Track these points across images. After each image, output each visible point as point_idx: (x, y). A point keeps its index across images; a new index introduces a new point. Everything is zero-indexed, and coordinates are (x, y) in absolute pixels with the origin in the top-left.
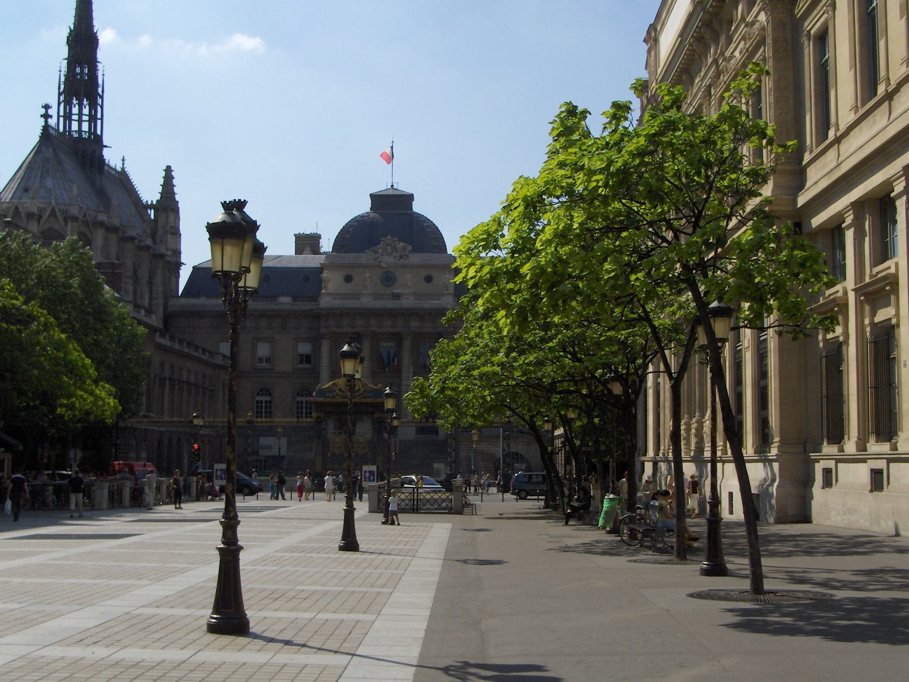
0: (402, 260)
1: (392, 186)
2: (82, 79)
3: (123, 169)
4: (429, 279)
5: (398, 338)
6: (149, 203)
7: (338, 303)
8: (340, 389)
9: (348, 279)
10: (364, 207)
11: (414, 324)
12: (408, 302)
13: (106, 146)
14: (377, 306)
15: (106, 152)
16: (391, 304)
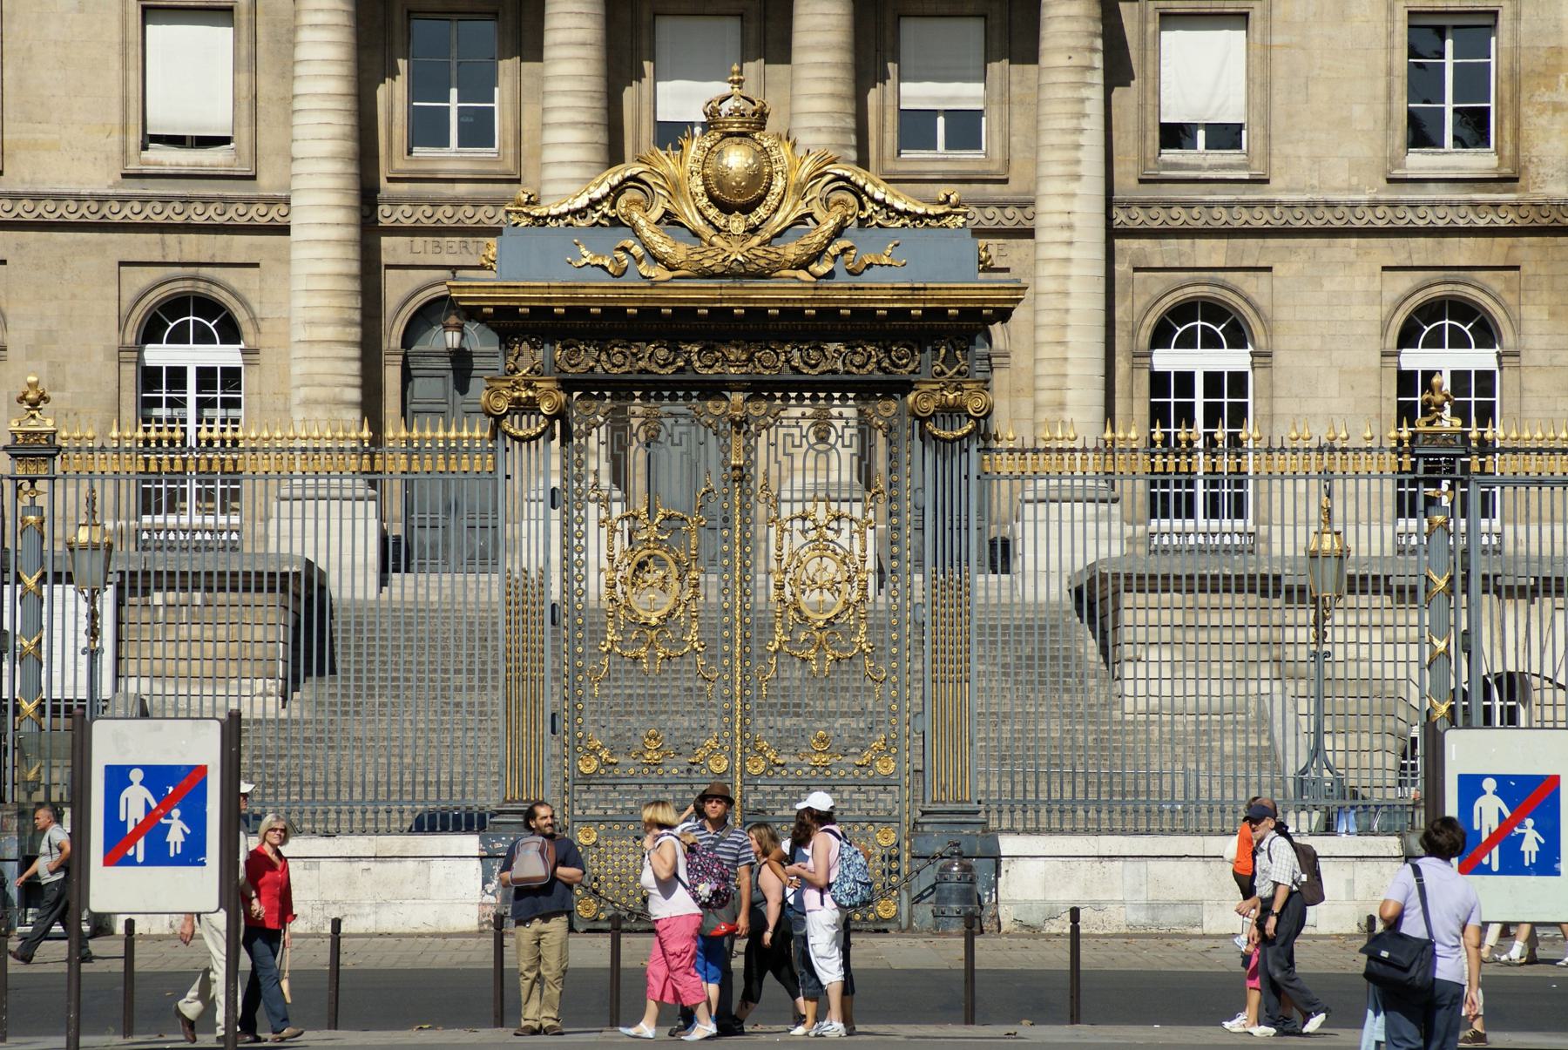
8: (670, 219)
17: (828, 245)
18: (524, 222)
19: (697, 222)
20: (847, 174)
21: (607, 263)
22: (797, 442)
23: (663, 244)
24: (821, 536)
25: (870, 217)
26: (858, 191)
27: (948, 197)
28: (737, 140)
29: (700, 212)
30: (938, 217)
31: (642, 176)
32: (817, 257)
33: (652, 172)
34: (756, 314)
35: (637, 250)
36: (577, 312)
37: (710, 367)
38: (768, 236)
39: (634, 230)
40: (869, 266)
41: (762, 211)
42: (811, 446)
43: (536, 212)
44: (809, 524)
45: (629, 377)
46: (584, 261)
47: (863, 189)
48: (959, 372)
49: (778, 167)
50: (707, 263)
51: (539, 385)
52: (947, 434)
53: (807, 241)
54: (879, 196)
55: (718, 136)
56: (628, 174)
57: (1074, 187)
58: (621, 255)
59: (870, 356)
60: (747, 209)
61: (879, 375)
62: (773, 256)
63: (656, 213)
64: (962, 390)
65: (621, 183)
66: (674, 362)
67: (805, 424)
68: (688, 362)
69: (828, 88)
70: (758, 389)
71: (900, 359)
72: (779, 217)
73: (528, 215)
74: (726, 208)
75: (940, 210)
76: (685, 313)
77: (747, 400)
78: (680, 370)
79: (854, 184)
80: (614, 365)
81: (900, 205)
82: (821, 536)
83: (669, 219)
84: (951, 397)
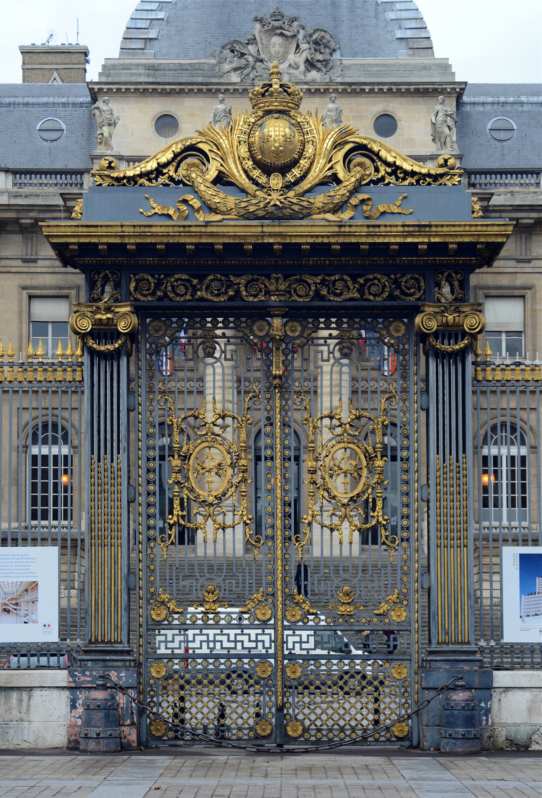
0: (314, 75)
4: (386, 125)
8: (221, 180)
17: (349, 198)
18: (108, 181)
20: (365, 142)
21: (171, 212)
22: (325, 356)
24: (345, 431)
25: (383, 179)
27: (446, 161)
28: (276, 115)
29: (246, 172)
30: (436, 178)
31: (200, 146)
34: (292, 249)
35: (196, 203)
36: (145, 249)
37: (255, 296)
38: (301, 190)
39: (191, 187)
40: (384, 213)
41: (296, 172)
42: (337, 360)
43: (115, 175)
44: (335, 422)
45: (190, 304)
46: (153, 211)
47: (377, 154)
48: (456, 300)
49: (309, 137)
50: (252, 209)
51: (117, 310)
52: (447, 347)
53: (332, 193)
54: (390, 159)
55: (260, 113)
56: (188, 143)
58: (184, 207)
59: (384, 287)
60: (284, 170)
61: (389, 303)
62: (305, 204)
63: (212, 174)
64: (459, 312)
65: (183, 151)
66: (226, 293)
67: (332, 342)
68: (238, 292)
70: (293, 313)
71: (409, 289)
72: (310, 177)
73: (109, 176)
75: (441, 171)
76: (234, 249)
77: (285, 325)
78: (231, 299)
79: (370, 150)
80: (178, 295)
82: (345, 431)
83: (221, 180)
84: (450, 317)
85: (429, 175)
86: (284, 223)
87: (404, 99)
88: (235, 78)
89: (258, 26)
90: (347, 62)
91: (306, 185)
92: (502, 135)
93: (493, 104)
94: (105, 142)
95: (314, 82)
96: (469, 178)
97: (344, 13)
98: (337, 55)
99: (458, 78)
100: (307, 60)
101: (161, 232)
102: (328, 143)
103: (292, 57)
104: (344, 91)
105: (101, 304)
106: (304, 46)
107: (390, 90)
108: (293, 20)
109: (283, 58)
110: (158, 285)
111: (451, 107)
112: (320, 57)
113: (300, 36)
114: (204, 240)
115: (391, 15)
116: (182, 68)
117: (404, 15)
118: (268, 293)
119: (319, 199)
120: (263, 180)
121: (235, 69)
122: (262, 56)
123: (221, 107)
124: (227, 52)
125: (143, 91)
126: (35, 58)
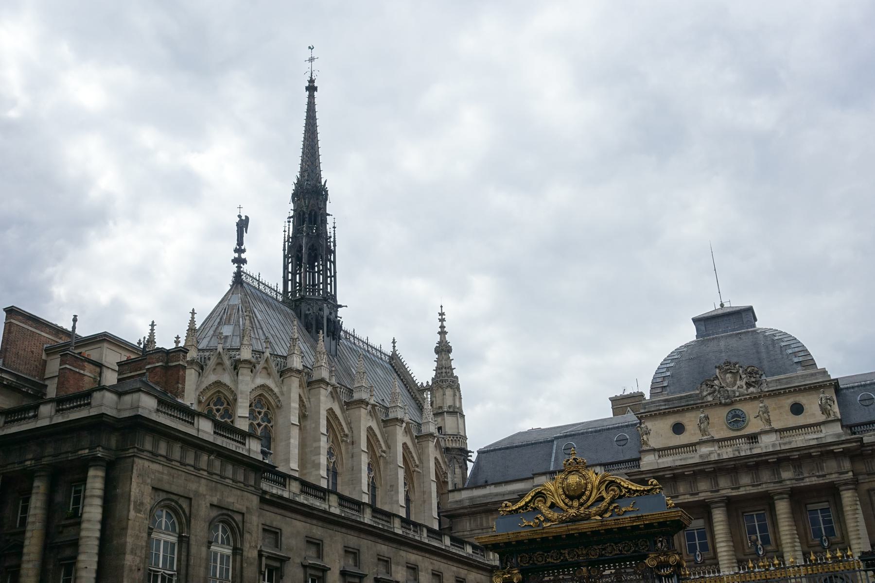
0: (751, 389)
1: (722, 305)
2: (310, 240)
3: (394, 352)
4: (797, 409)
5: (767, 500)
6: (425, 385)
7: (667, 461)
8: (553, 506)
9: (678, 429)
10: (690, 334)
11: (786, 474)
12: (768, 443)
13: (341, 306)
14: (725, 457)
15: (341, 312)
16: (745, 450)
19: (562, 505)
23: (551, 514)
25: (624, 495)
26: (619, 486)
30: (648, 491)
32: (606, 511)
33: (545, 490)
34: (582, 535)
36: (519, 543)
41: (584, 497)
57: (859, 541)
60: (579, 497)
63: (549, 504)
69: (787, 523)
70: (592, 564)
74: (572, 498)
75: (649, 487)
76: (557, 538)
81: (634, 488)
85: (644, 490)
86: (577, 523)
87: (805, 394)
88: (710, 398)
89: (717, 370)
90: (769, 379)
91: (589, 503)
92: (867, 402)
93: (858, 386)
94: (645, 443)
95: (752, 393)
96: (851, 430)
97: (764, 355)
98: (764, 377)
99: (832, 378)
100: (746, 383)
101: (525, 534)
102: (597, 482)
103: (738, 383)
104: (770, 395)
105: (505, 571)
106: (743, 376)
107: (795, 390)
108: (735, 364)
109: (734, 384)
110: (531, 558)
111: (831, 393)
112: (753, 380)
113: (741, 372)
114: (544, 536)
115: (790, 351)
116: (681, 398)
117: (797, 350)
118: (579, 556)
119: (594, 510)
120: (570, 503)
121: (709, 394)
122: (723, 385)
123: (702, 415)
124: (704, 386)
125: (663, 414)
126: (619, 403)
